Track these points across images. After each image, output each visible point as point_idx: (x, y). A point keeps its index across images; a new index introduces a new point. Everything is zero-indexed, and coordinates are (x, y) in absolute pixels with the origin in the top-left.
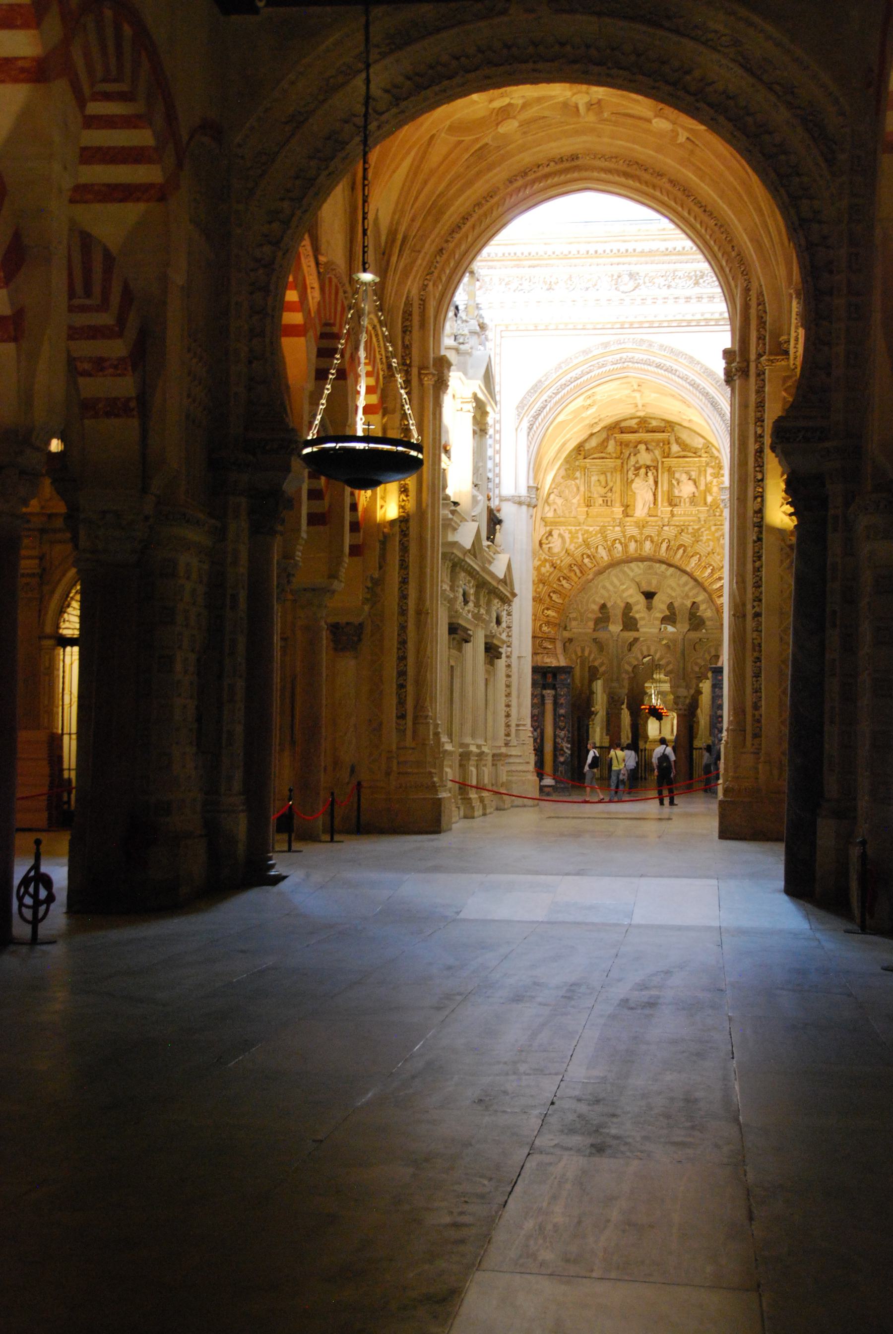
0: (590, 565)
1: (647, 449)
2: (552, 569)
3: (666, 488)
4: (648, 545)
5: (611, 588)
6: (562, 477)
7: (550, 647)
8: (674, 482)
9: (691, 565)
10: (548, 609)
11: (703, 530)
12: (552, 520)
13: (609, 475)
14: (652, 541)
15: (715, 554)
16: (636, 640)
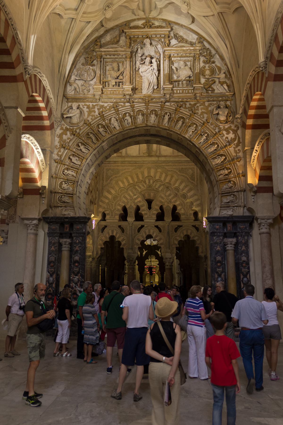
0: (103, 133)
1: (151, 44)
2: (73, 136)
3: (166, 72)
4: (153, 118)
5: (128, 197)
6: (83, 64)
7: (68, 201)
8: (173, 67)
9: (189, 134)
10: (68, 169)
11: (198, 105)
12: (73, 97)
13: (121, 65)
14: (156, 115)
15: (209, 124)
16: (142, 226)
